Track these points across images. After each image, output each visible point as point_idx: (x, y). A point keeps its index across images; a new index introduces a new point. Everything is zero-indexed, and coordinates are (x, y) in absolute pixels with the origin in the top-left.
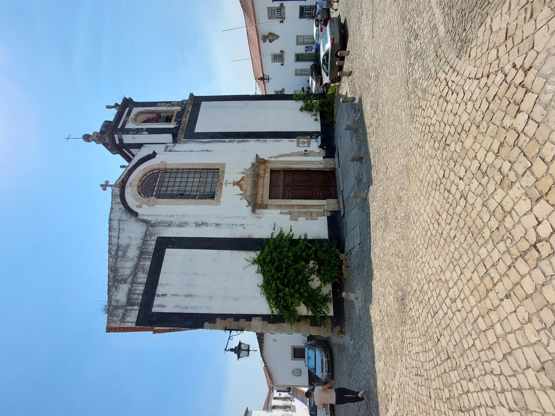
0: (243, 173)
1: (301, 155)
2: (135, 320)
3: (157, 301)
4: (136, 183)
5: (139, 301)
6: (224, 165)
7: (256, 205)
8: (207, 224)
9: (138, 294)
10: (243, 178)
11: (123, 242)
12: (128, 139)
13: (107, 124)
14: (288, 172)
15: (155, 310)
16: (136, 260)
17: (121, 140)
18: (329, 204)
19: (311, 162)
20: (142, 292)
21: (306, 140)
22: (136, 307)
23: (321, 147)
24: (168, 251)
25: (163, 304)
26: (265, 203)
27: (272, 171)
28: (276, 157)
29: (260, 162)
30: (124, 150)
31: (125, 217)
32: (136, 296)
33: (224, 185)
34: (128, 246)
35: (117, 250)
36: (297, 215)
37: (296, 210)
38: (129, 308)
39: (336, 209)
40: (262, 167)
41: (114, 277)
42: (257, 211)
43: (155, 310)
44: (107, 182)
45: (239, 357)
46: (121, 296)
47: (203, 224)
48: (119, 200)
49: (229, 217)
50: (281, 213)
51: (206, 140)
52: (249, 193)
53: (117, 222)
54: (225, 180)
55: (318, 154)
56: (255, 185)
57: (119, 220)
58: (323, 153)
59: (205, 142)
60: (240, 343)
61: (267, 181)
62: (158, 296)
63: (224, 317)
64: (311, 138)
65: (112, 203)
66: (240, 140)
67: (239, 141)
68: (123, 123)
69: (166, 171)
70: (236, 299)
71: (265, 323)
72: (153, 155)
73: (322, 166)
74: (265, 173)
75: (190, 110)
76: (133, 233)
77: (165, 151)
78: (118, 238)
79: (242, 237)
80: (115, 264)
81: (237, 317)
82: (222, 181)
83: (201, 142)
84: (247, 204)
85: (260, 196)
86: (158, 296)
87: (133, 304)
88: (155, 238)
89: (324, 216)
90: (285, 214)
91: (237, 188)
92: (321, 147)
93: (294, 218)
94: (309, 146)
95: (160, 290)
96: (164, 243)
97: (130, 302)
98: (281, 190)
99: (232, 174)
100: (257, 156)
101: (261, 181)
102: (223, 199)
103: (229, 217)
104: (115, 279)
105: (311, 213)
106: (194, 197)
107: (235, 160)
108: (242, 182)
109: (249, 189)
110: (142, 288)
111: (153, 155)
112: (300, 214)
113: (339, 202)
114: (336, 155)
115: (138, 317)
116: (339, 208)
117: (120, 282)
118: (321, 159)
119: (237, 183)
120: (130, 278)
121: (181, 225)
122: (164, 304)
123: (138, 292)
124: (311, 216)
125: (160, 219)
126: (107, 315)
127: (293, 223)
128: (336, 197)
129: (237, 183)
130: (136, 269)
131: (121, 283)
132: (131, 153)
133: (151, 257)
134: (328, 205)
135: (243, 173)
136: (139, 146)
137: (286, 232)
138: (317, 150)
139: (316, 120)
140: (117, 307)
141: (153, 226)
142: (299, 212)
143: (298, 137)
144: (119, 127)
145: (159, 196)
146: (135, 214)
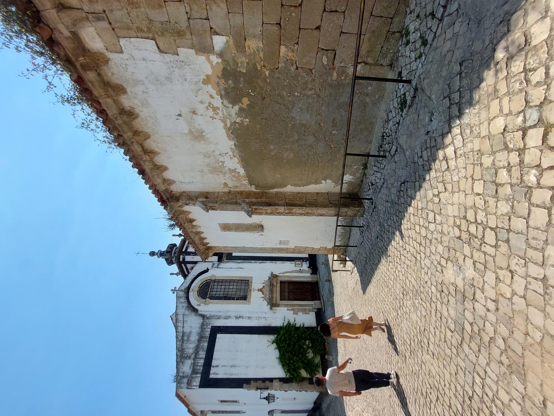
0: (264, 283)
1: (297, 272)
2: (198, 384)
3: (213, 370)
4: (197, 289)
5: (201, 371)
6: (251, 278)
7: (273, 305)
8: (242, 317)
9: (200, 366)
10: (264, 286)
11: (187, 330)
12: (188, 258)
13: (172, 246)
14: (290, 283)
15: (212, 376)
16: (196, 342)
17: (184, 259)
18: (315, 304)
19: (304, 277)
20: (202, 364)
22: (199, 375)
23: (309, 267)
24: (219, 336)
25: (217, 372)
26: (278, 303)
27: (281, 282)
28: (283, 273)
29: (274, 277)
30: (183, 265)
31: (187, 312)
32: (198, 367)
34: (190, 333)
35: (183, 336)
36: (297, 311)
37: (296, 308)
38: (195, 376)
40: (275, 280)
41: (181, 355)
42: (273, 308)
43: (212, 376)
44: (176, 288)
45: (269, 403)
46: (187, 368)
47: (240, 317)
48: (183, 300)
49: (256, 313)
50: (288, 310)
52: (268, 297)
53: (182, 316)
56: (271, 291)
57: (183, 315)
58: (310, 271)
59: (239, 263)
60: (269, 394)
61: (278, 289)
62: (213, 367)
63: (256, 380)
64: (303, 261)
65: (177, 303)
69: (215, 281)
70: (263, 368)
71: (281, 383)
72: (207, 271)
73: (310, 280)
76: (193, 324)
77: (213, 266)
78: (183, 327)
79: (265, 325)
80: (182, 345)
81: (264, 380)
83: (237, 262)
84: (267, 304)
86: (213, 367)
87: (197, 373)
88: (210, 327)
90: (289, 310)
91: (260, 293)
92: (309, 267)
93: (296, 313)
94: (302, 267)
95: (214, 363)
96: (216, 330)
97: (194, 372)
98: (286, 294)
99: (257, 284)
101: (275, 289)
103: (256, 313)
104: (181, 356)
105: (305, 309)
106: (233, 299)
107: (258, 274)
108: (263, 289)
110: (202, 361)
111: (207, 271)
112: (299, 311)
113: (321, 303)
114: (318, 272)
115: (200, 382)
117: (186, 358)
118: (309, 275)
119: (260, 290)
120: (193, 356)
121: (227, 318)
122: (217, 373)
123: (200, 364)
124: (305, 312)
125: (212, 314)
126: (176, 383)
127: (295, 316)
128: (320, 300)
129: (260, 290)
130: (197, 349)
131: (186, 359)
132: (186, 266)
133: (208, 340)
134: (315, 304)
135: (264, 283)
136: (195, 263)
137: (292, 322)
138: (307, 269)
140: (183, 377)
141: (208, 318)
142: (298, 309)
144: (184, 250)
145: (211, 298)
146: (195, 310)
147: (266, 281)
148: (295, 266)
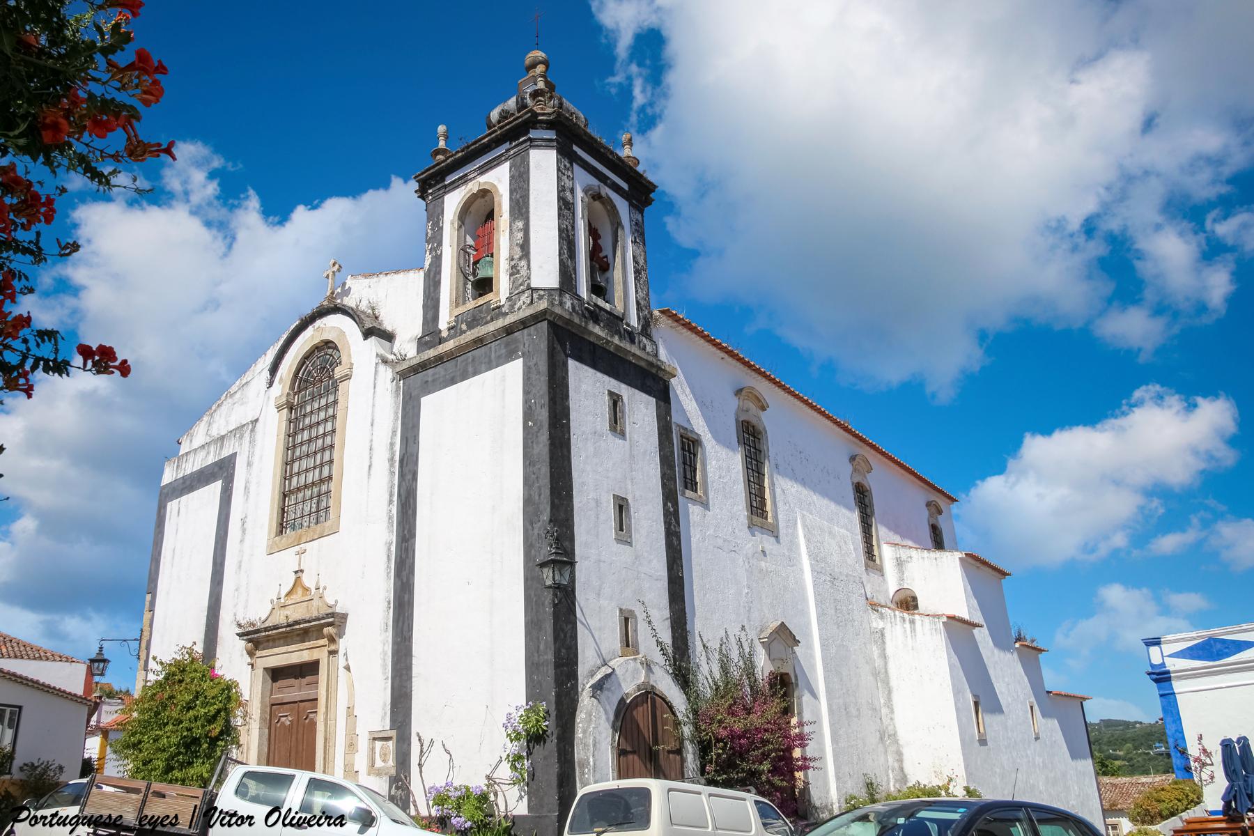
10: (306, 590)
29: (325, 627)
33: (297, 549)
47: (244, 531)
66: (393, 548)
83: (394, 432)
129: (298, 580)
143: (393, 733)
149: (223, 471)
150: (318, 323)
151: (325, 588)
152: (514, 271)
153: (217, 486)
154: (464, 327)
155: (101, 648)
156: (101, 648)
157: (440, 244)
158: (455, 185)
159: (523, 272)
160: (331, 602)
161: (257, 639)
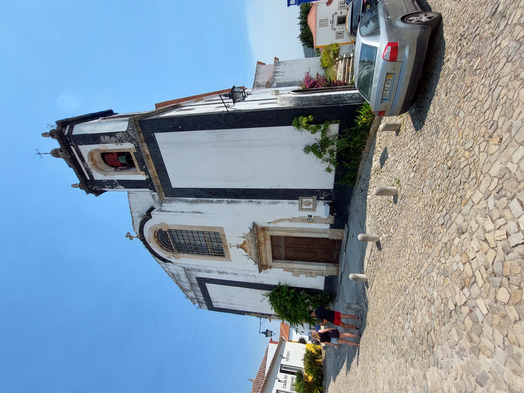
0: (244, 237)
8: (227, 273)
10: (245, 243)
19: (315, 231)
21: (311, 200)
28: (274, 222)
33: (229, 247)
39: (335, 274)
47: (223, 272)
51: (191, 199)
54: (228, 242)
55: (324, 221)
58: (331, 220)
59: (191, 202)
64: (318, 199)
66: (229, 200)
67: (228, 201)
68: (87, 172)
73: (326, 236)
74: (265, 240)
75: (147, 151)
82: (226, 244)
85: (264, 259)
89: (322, 275)
94: (314, 210)
98: (283, 251)
100: (254, 225)
101: (262, 247)
102: (232, 257)
103: (242, 270)
108: (245, 246)
109: (253, 252)
113: (338, 270)
116: (337, 274)
118: (328, 226)
129: (241, 247)
135: (244, 237)
139: (329, 170)
143: (300, 198)
147: (247, 235)
148: (301, 209)
149: (202, 282)
150: (148, 242)
151: (244, 234)
152: (121, 141)
153: (209, 286)
154: (144, 167)
155: (263, 333)
156: (263, 333)
157: (113, 181)
158: (91, 176)
159: (121, 135)
160: (249, 231)
161: (262, 267)
